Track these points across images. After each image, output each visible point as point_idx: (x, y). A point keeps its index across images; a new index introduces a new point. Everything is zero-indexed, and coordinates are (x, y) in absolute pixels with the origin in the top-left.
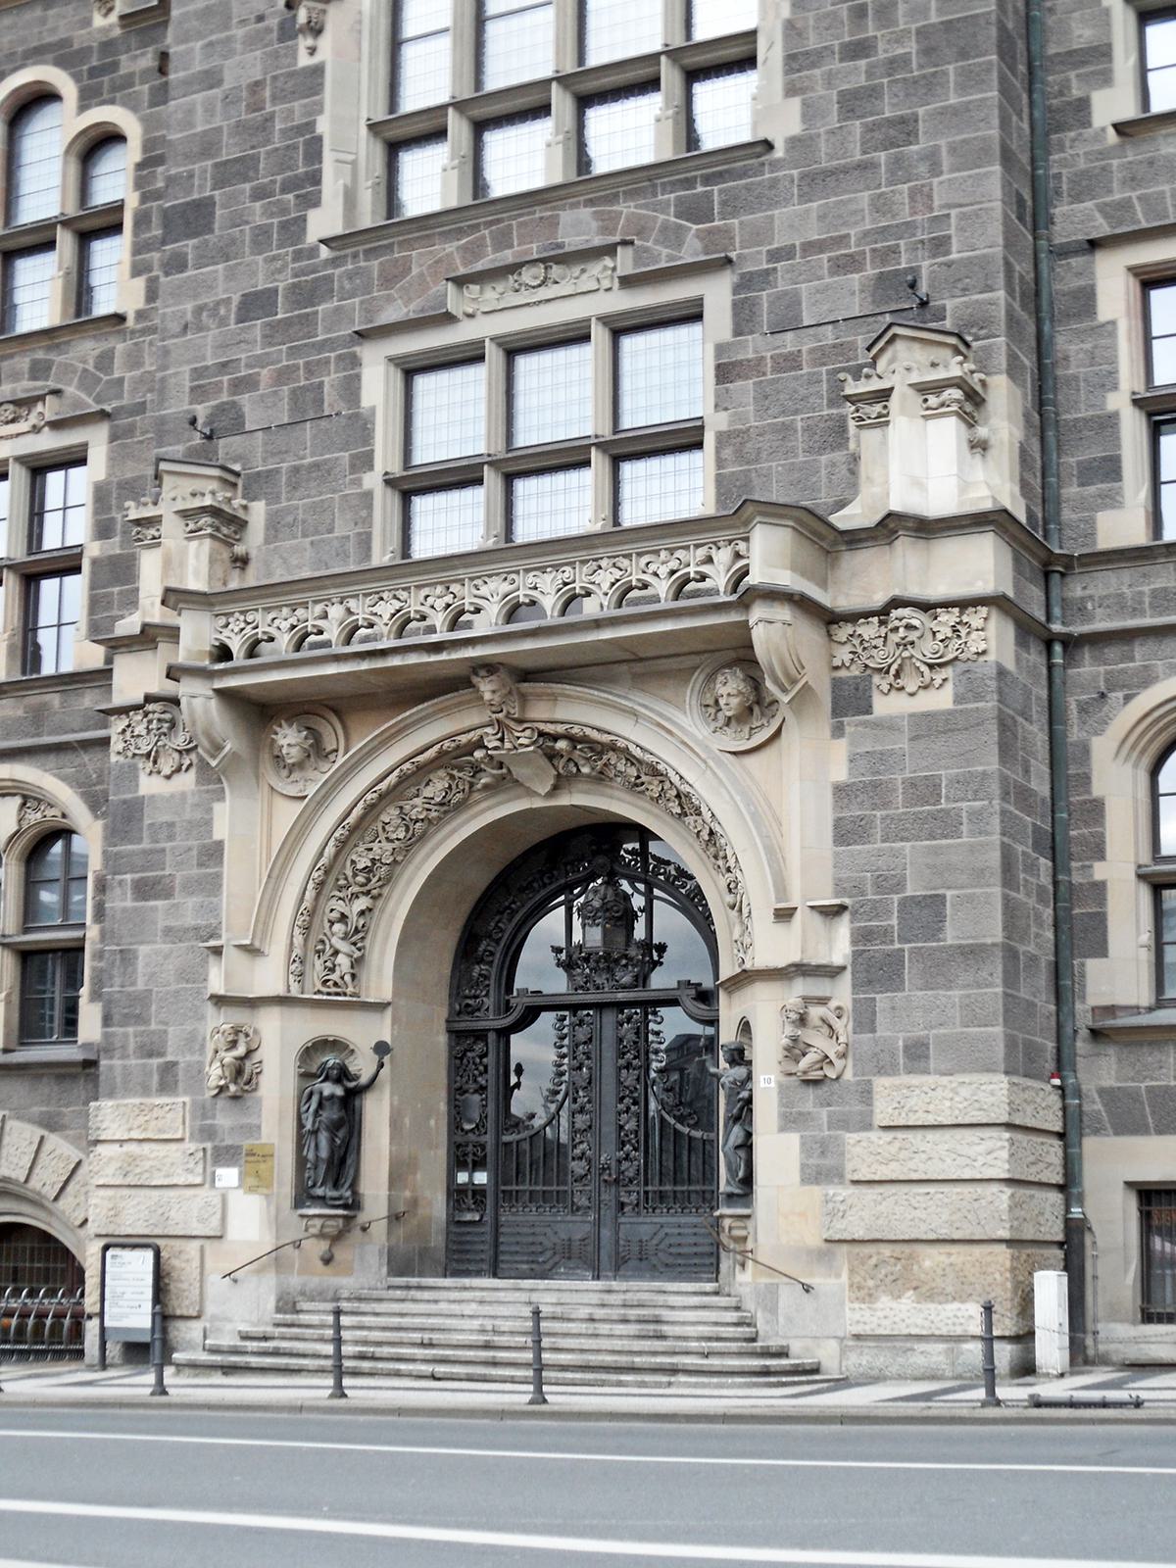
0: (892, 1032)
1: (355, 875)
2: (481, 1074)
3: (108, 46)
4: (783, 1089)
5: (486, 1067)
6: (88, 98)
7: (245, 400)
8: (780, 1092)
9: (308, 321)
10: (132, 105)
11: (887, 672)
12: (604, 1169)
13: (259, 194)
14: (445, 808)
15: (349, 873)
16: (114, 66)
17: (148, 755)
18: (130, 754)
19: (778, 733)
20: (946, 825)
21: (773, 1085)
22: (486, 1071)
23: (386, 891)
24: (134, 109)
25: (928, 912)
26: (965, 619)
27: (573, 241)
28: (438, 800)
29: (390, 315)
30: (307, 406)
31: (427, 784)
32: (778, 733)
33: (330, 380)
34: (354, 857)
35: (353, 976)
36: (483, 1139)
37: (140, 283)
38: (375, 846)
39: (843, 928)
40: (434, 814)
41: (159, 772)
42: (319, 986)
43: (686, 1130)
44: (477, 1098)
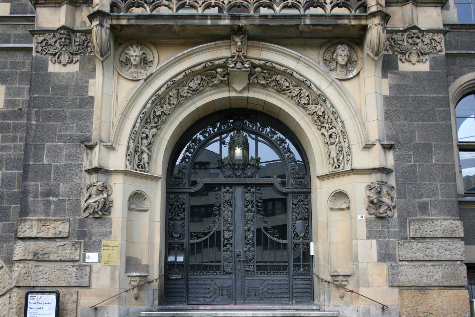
1: (154, 118)
2: (182, 212)
4: (368, 221)
5: (184, 209)
8: (366, 222)
11: (405, 54)
12: (238, 255)
14: (194, 93)
15: (152, 117)
17: (55, 55)
18: (44, 53)
19: (358, 74)
21: (364, 218)
22: (184, 211)
23: (162, 126)
26: (434, 38)
28: (194, 88)
31: (191, 81)
32: (358, 74)
34: (156, 110)
35: (148, 163)
36: (182, 241)
38: (164, 106)
39: (391, 155)
40: (189, 95)
41: (60, 63)
42: (136, 167)
43: (275, 239)
44: (180, 223)
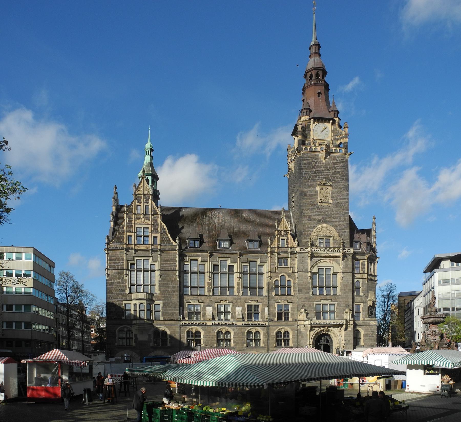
0: (347, 347)
3: (290, 274)
6: (289, 277)
7: (305, 304)
9: (310, 300)
10: (292, 279)
13: (306, 290)
16: (291, 275)
20: (350, 336)
24: (293, 279)
25: (349, 341)
27: (328, 299)
29: (316, 301)
30: (310, 305)
33: (312, 304)
37: (294, 293)
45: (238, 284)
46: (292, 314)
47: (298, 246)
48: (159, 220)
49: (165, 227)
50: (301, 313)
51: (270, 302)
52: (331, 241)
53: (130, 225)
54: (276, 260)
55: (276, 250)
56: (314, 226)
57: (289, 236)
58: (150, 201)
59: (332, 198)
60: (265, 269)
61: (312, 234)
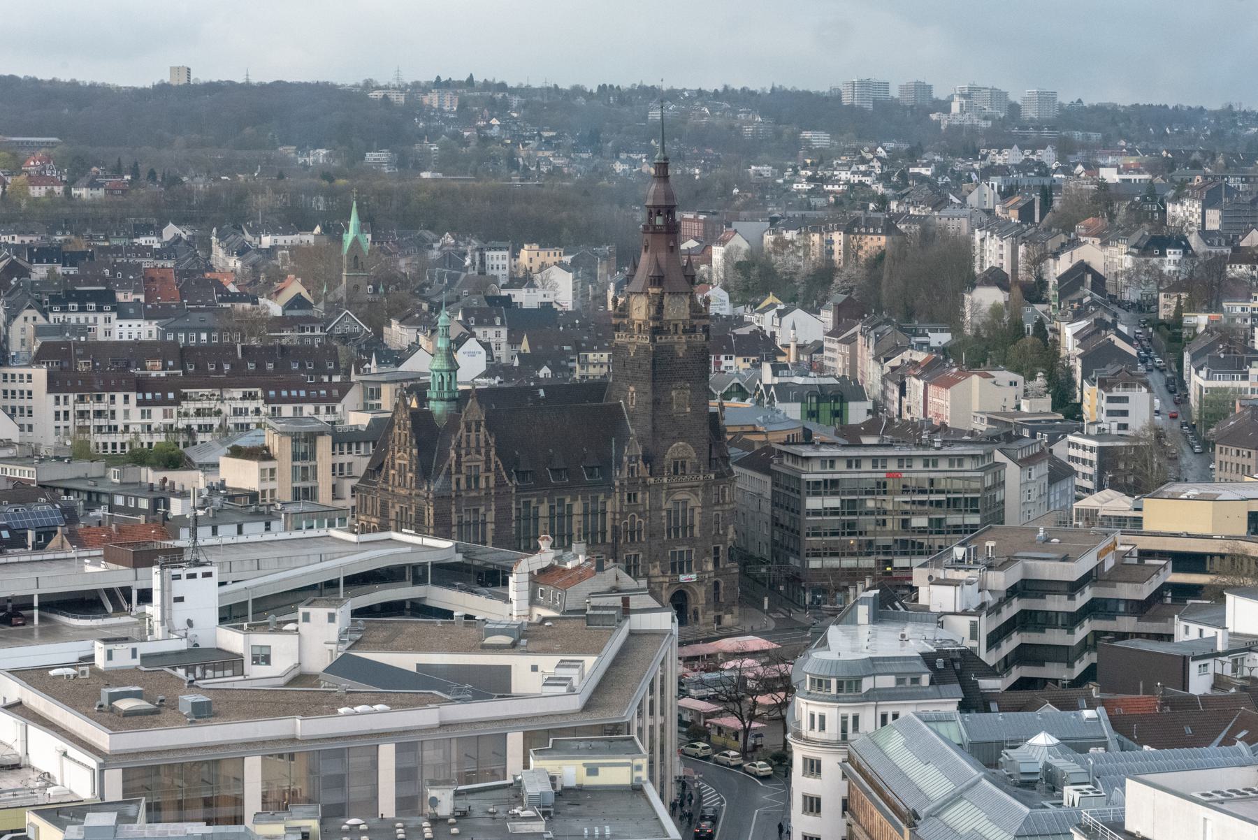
45: (579, 530)
46: (643, 567)
47: (651, 475)
48: (492, 453)
49: (499, 463)
50: (656, 567)
51: (618, 554)
52: (688, 465)
53: (459, 463)
54: (626, 497)
55: (626, 483)
56: (670, 446)
57: (640, 462)
58: (482, 429)
59: (690, 405)
60: (609, 508)
61: (667, 457)
